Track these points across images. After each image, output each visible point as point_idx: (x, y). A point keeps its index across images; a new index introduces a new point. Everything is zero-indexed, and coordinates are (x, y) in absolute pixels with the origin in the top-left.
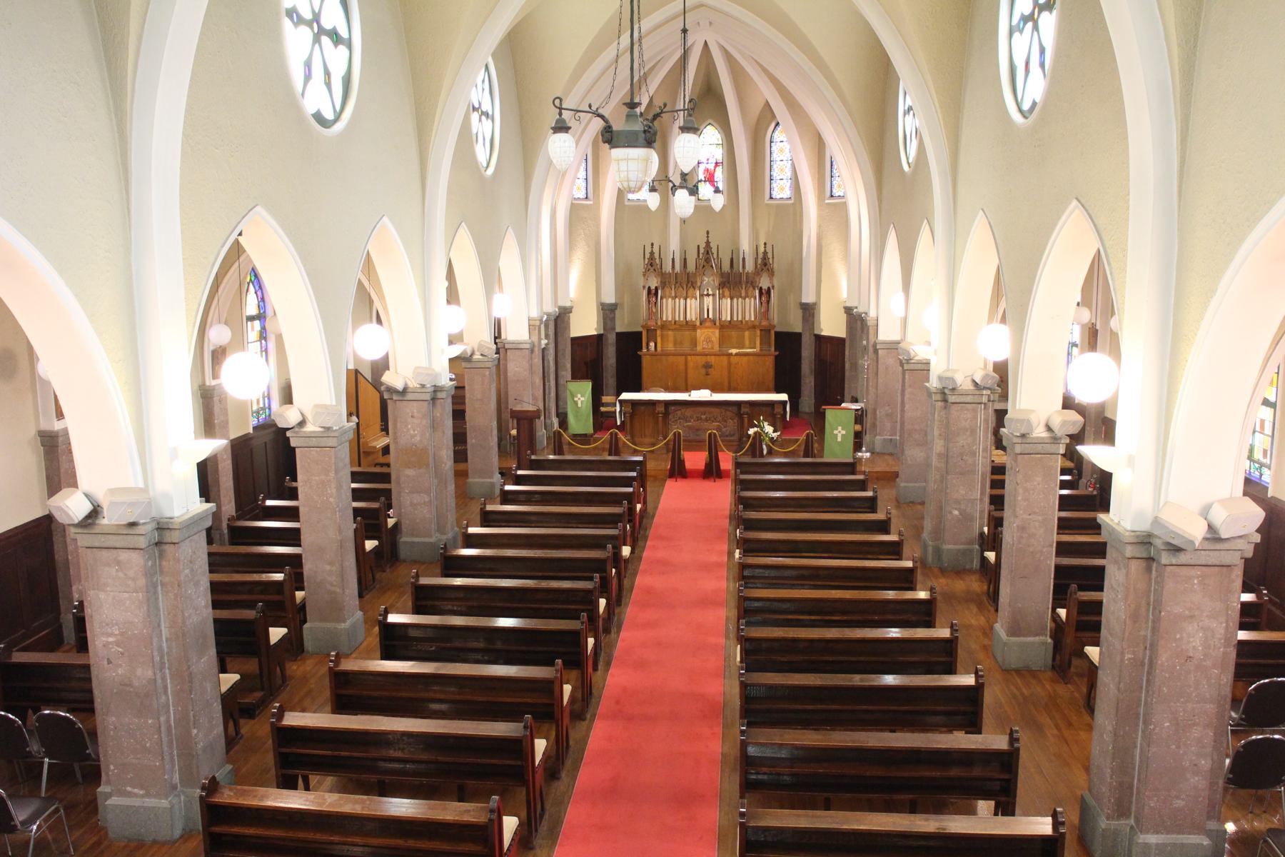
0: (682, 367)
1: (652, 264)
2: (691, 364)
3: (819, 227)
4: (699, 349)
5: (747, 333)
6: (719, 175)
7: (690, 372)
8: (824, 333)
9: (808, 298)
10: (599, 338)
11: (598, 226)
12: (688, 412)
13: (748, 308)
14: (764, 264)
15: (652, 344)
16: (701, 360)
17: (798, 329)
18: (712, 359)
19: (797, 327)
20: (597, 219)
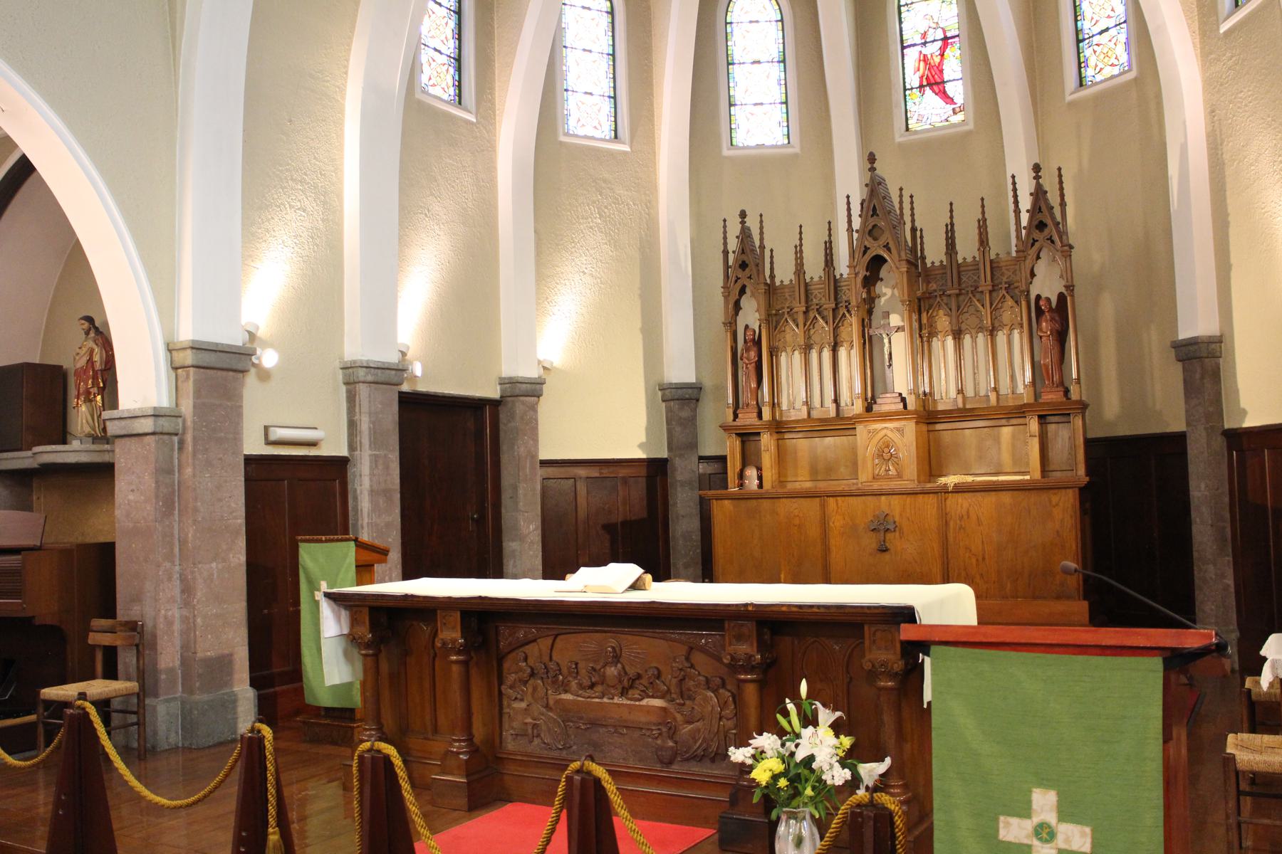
0: (814, 531)
1: (744, 266)
2: (836, 523)
3: (1212, 112)
4: (864, 476)
5: (1006, 432)
6: (953, 68)
7: (835, 542)
8: (1249, 423)
9: (1196, 323)
10: (655, 470)
11: (650, 205)
12: (573, 648)
13: (998, 364)
14: (1044, 224)
15: (751, 473)
16: (863, 509)
17: (1176, 424)
18: (894, 506)
19: (1168, 411)
20: (647, 189)
